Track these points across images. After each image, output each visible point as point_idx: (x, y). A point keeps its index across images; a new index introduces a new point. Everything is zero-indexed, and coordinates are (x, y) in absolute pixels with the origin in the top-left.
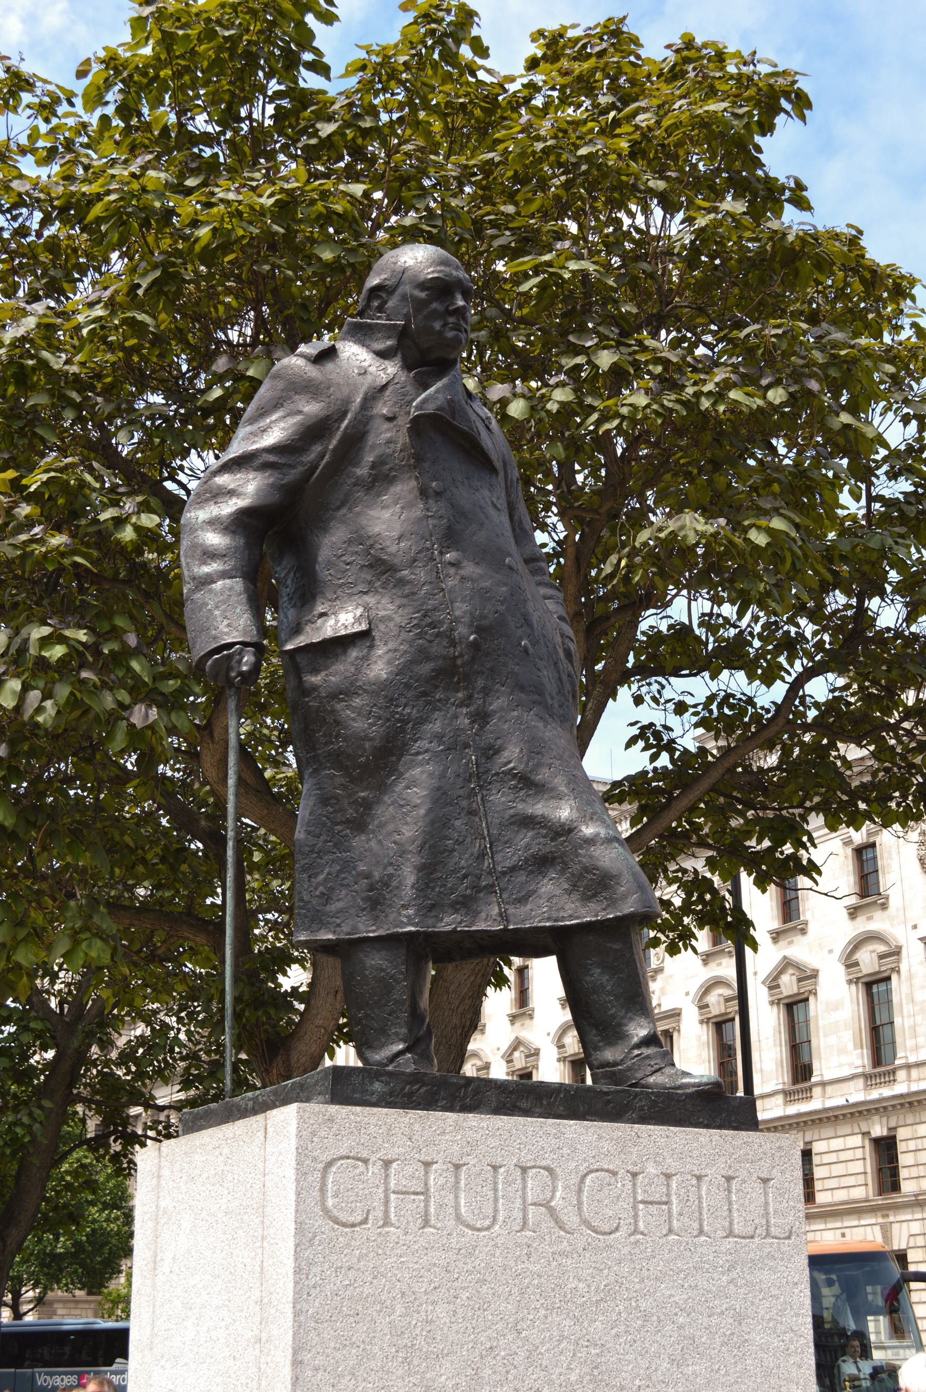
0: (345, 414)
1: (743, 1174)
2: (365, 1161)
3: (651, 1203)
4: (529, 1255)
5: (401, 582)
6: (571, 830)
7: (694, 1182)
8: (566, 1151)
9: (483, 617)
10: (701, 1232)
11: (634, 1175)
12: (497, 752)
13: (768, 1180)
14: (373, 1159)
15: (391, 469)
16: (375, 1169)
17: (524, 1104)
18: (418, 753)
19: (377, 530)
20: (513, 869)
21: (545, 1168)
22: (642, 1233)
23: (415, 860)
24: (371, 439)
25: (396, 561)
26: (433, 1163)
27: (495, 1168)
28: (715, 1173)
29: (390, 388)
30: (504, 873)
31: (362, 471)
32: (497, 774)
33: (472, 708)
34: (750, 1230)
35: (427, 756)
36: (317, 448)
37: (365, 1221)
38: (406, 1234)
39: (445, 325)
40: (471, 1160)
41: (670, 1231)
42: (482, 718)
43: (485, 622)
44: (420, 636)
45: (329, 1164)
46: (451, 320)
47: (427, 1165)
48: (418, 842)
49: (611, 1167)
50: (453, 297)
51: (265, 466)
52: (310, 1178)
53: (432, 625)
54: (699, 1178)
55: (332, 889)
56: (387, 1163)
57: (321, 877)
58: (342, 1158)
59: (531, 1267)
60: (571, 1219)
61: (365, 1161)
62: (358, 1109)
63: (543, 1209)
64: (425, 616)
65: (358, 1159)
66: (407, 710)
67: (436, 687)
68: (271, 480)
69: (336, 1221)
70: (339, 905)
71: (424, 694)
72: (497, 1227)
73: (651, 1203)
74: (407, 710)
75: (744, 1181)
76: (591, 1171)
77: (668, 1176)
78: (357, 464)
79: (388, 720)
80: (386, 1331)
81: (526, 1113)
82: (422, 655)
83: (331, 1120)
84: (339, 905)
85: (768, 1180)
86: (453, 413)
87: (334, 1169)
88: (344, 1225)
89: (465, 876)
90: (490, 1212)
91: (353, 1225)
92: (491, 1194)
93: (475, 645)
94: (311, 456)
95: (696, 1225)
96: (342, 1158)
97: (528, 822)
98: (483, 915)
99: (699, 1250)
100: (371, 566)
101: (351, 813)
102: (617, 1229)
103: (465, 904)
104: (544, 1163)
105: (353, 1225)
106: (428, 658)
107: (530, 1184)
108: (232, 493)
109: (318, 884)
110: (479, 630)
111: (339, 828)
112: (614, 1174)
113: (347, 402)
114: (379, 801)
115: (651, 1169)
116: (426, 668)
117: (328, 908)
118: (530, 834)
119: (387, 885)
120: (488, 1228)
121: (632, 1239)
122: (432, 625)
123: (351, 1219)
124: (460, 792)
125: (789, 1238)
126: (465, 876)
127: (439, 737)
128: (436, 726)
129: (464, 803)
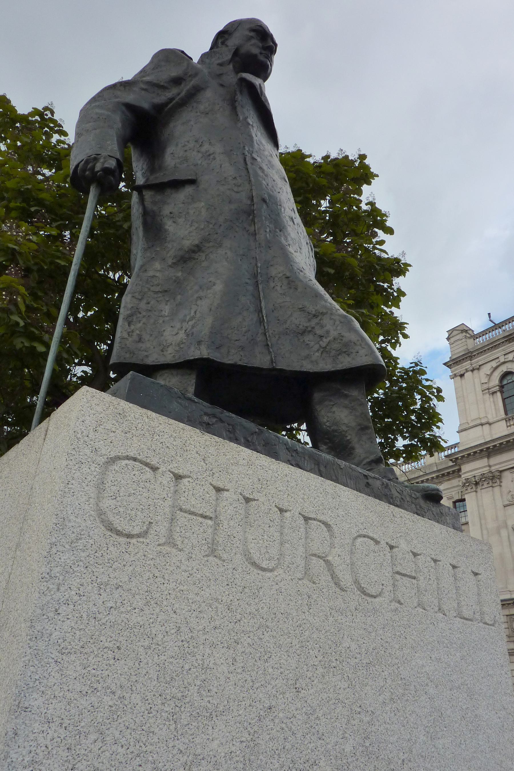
2: (154, 469)
4: (309, 606)
14: (162, 468)
21: (324, 523)
22: (399, 602)
26: (223, 490)
38: (189, 558)
47: (218, 490)
52: (85, 469)
58: (128, 458)
61: (154, 469)
65: (147, 464)
69: (111, 528)
80: (153, 674)
83: (122, 415)
88: (119, 533)
90: (274, 552)
96: (128, 458)
104: (322, 518)
105: (129, 536)
115: (403, 545)
117: (140, 345)
120: (271, 571)
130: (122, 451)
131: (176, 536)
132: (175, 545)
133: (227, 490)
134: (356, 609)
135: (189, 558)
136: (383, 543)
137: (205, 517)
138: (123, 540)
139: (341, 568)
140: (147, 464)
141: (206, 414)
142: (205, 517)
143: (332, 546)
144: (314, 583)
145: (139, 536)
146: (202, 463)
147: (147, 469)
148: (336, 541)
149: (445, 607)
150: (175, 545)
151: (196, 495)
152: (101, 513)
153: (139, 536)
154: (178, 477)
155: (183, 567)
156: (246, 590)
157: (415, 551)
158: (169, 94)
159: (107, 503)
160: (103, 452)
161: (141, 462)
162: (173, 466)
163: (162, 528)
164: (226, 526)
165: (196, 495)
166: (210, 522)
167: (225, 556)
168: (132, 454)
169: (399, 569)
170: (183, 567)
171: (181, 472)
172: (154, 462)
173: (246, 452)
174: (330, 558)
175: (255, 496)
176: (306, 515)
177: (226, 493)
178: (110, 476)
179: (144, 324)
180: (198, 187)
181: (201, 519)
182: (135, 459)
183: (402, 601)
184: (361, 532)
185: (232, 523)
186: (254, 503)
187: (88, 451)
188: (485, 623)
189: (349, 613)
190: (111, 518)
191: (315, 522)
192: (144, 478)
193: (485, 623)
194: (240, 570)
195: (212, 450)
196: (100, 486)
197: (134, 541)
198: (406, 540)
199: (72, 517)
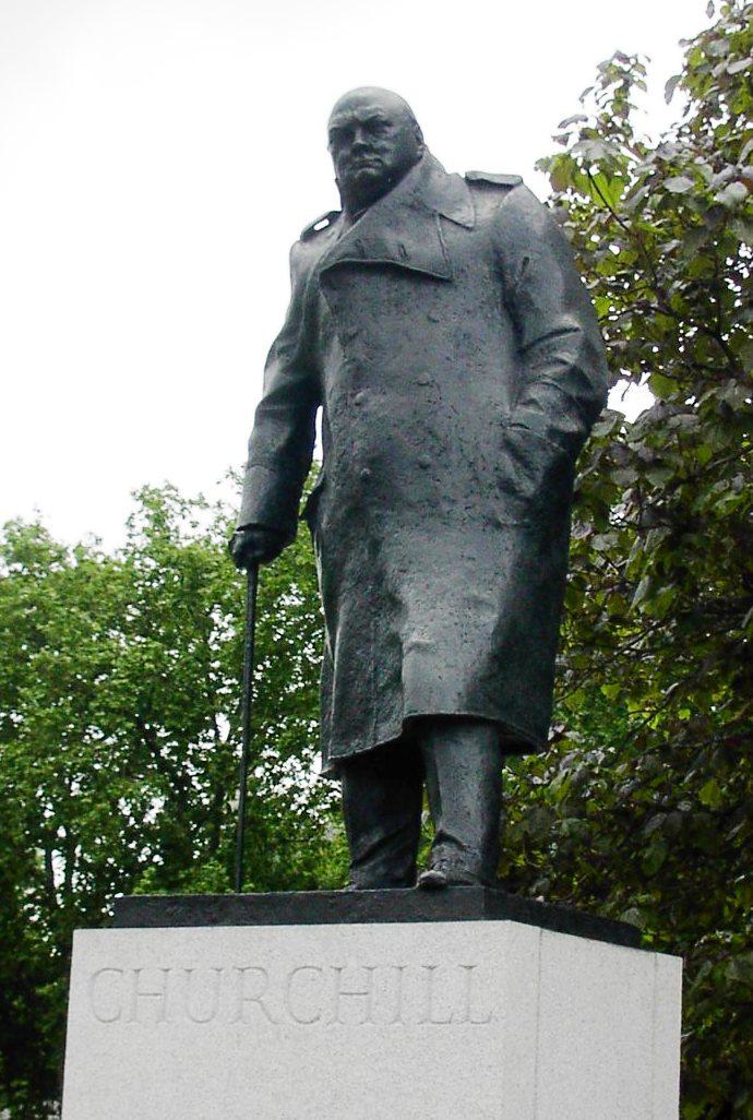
2: (121, 971)
4: (239, 1042)
7: (395, 972)
8: (276, 952)
13: (471, 967)
27: (219, 970)
34: (446, 1016)
41: (369, 1019)
42: (375, 546)
54: (401, 968)
56: (138, 971)
58: (104, 970)
63: (255, 1003)
75: (445, 971)
76: (298, 969)
77: (370, 969)
85: (471, 967)
86: (362, 254)
87: (98, 979)
88: (104, 1021)
93: (365, 479)
96: (104, 970)
102: (318, 1019)
104: (256, 964)
105: (110, 1021)
113: (308, 269)
115: (352, 963)
120: (208, 1021)
125: (488, 1021)
128: (348, 567)
142: (156, 995)
145: (115, 1019)
154: (138, 971)
166: (159, 997)
167: (170, 1019)
168: (105, 967)
172: (119, 967)
174: (262, 999)
181: (152, 997)
198: (358, 957)
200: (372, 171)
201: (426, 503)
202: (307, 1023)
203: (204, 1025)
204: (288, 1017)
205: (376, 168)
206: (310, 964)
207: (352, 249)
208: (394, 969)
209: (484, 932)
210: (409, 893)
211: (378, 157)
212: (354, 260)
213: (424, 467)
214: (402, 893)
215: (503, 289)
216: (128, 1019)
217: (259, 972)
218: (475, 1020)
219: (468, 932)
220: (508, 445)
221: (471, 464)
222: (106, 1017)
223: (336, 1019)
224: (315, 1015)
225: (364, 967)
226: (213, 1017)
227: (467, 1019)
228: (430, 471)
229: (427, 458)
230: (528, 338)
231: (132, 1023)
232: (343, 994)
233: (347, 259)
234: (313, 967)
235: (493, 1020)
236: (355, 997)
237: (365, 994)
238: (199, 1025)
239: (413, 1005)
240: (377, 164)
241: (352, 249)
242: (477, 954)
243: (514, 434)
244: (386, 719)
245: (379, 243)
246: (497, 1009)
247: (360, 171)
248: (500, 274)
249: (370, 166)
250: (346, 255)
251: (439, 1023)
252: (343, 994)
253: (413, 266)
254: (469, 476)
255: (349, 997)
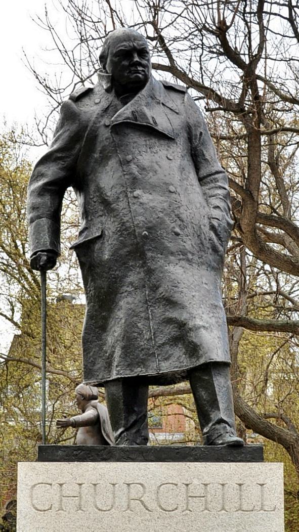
0: (87, 127)
1: (247, 482)
2: (51, 485)
3: (196, 497)
4: (129, 521)
5: (113, 210)
6: (185, 324)
7: (220, 486)
9: (151, 222)
10: (223, 509)
11: (187, 485)
12: (157, 288)
13: (263, 484)
14: (53, 483)
15: (108, 152)
16: (56, 487)
17: (132, 456)
18: (123, 293)
19: (103, 186)
20: (163, 344)
23: (122, 344)
24: (100, 139)
25: (111, 199)
28: (232, 484)
29: (110, 109)
30: (159, 347)
31: (96, 155)
32: (158, 299)
33: (145, 268)
34: (251, 508)
35: (126, 294)
36: (78, 147)
37: (51, 508)
38: (69, 513)
39: (130, 72)
40: (101, 482)
41: (206, 509)
43: (150, 225)
44: (121, 235)
45: (35, 486)
46: (133, 69)
47: (80, 485)
48: (122, 336)
49: (174, 482)
50: (133, 57)
51: (57, 159)
52: (24, 492)
53: (126, 230)
54: (223, 485)
55: (95, 359)
56: (61, 485)
57: (92, 353)
58: (39, 484)
59: (130, 526)
60: (153, 505)
61: (51, 485)
62: (47, 463)
64: (122, 225)
65: (47, 484)
66: (117, 273)
67: (130, 259)
68: (60, 166)
70: (99, 366)
71: (124, 264)
72: (113, 509)
73: (196, 497)
74: (117, 273)
75: (249, 486)
76: (164, 484)
77: (206, 485)
78: (94, 152)
79: (109, 278)
81: (133, 460)
82: (123, 244)
83: (34, 468)
84: (99, 366)
85: (263, 484)
86: (136, 119)
87: (35, 488)
88: (41, 511)
89: (143, 350)
90: (109, 503)
91: (45, 511)
92: (111, 496)
93: (145, 237)
94: (75, 152)
95: (220, 507)
96: (39, 484)
97: (169, 321)
98: (151, 367)
99: (221, 517)
100: (102, 203)
101: (100, 323)
102: (176, 509)
103: (143, 363)
104: (138, 482)
105: (45, 511)
106: (125, 246)
107: (132, 490)
108: (42, 175)
109: (90, 357)
110: (149, 229)
111: (97, 330)
112: (176, 485)
114: (110, 317)
115: (196, 482)
116: (123, 252)
118: (171, 327)
119: (112, 356)
120: (109, 510)
121: (184, 513)
122: (126, 230)
123: (43, 508)
124: (141, 310)
125: (274, 510)
126: (143, 350)
127: (131, 284)
128: (129, 280)
129: (143, 315)
130: (37, 482)
131: (63, 506)
132: (63, 510)
133: (84, 483)
134: (158, 518)
135: (69, 513)
136: (179, 484)
137: (75, 497)
138: (42, 512)
139: (149, 502)
140: (47, 484)
141: (75, 450)
142: (75, 497)
143: (145, 493)
144: (132, 511)
145: (48, 510)
146: (71, 476)
147: (47, 485)
148: (147, 490)
149: (226, 508)
150: (63, 510)
151: (69, 490)
152: (33, 506)
153: (48, 510)
154: (61, 485)
155: (67, 517)
156: (96, 520)
157: (205, 483)
158: (75, 152)
159: (35, 501)
160: (29, 484)
161: (45, 483)
162: (58, 481)
163: (56, 505)
164: (84, 497)
165: (69, 490)
166: (77, 498)
167: (85, 509)
168: (40, 482)
169: (190, 494)
170: (67, 517)
171: (62, 483)
172: (50, 482)
173: (91, 465)
174: (142, 499)
175: (98, 482)
176: (127, 483)
177: (83, 485)
178: (34, 492)
179: (94, 352)
180: (104, 239)
181: (72, 498)
182: (42, 483)
183: (191, 510)
184: (163, 482)
185: (87, 496)
186: (98, 485)
187: (24, 486)
188: (265, 511)
189: (153, 520)
190: (36, 506)
191: (133, 485)
192: (46, 489)
193: (265, 511)
194: (92, 513)
195: (74, 469)
196: (31, 497)
197: (46, 512)
198: (198, 479)
199: (23, 509)
200: (140, 76)
201: (180, 253)
202: (170, 511)
203: (106, 512)
204: (158, 508)
205: (142, 75)
206: (171, 482)
207: (130, 116)
208: (184, 485)
209: (269, 468)
210: (222, 448)
211: (144, 69)
212: (132, 121)
213: (177, 234)
214: (219, 447)
215: (191, 147)
216: (57, 509)
217: (140, 486)
218: (266, 509)
219: (261, 467)
220: (213, 228)
221: (199, 236)
222: (39, 507)
223: (187, 509)
224: (175, 507)
225: (202, 484)
226: (112, 508)
227: (262, 509)
228: (180, 237)
229: (177, 230)
230: (203, 173)
231: (60, 511)
232: (190, 497)
233: (129, 121)
234: (172, 484)
235: (276, 510)
236: (197, 498)
237: (204, 497)
238: (103, 512)
239: (231, 502)
240: (143, 73)
241: (130, 116)
242: (266, 478)
243: (215, 223)
244: (166, 359)
245: (144, 116)
246: (279, 504)
247: (135, 75)
248: (190, 139)
249: (140, 73)
250: (128, 118)
251: (247, 511)
252: (190, 497)
253: (159, 128)
254: (199, 242)
255: (194, 498)
